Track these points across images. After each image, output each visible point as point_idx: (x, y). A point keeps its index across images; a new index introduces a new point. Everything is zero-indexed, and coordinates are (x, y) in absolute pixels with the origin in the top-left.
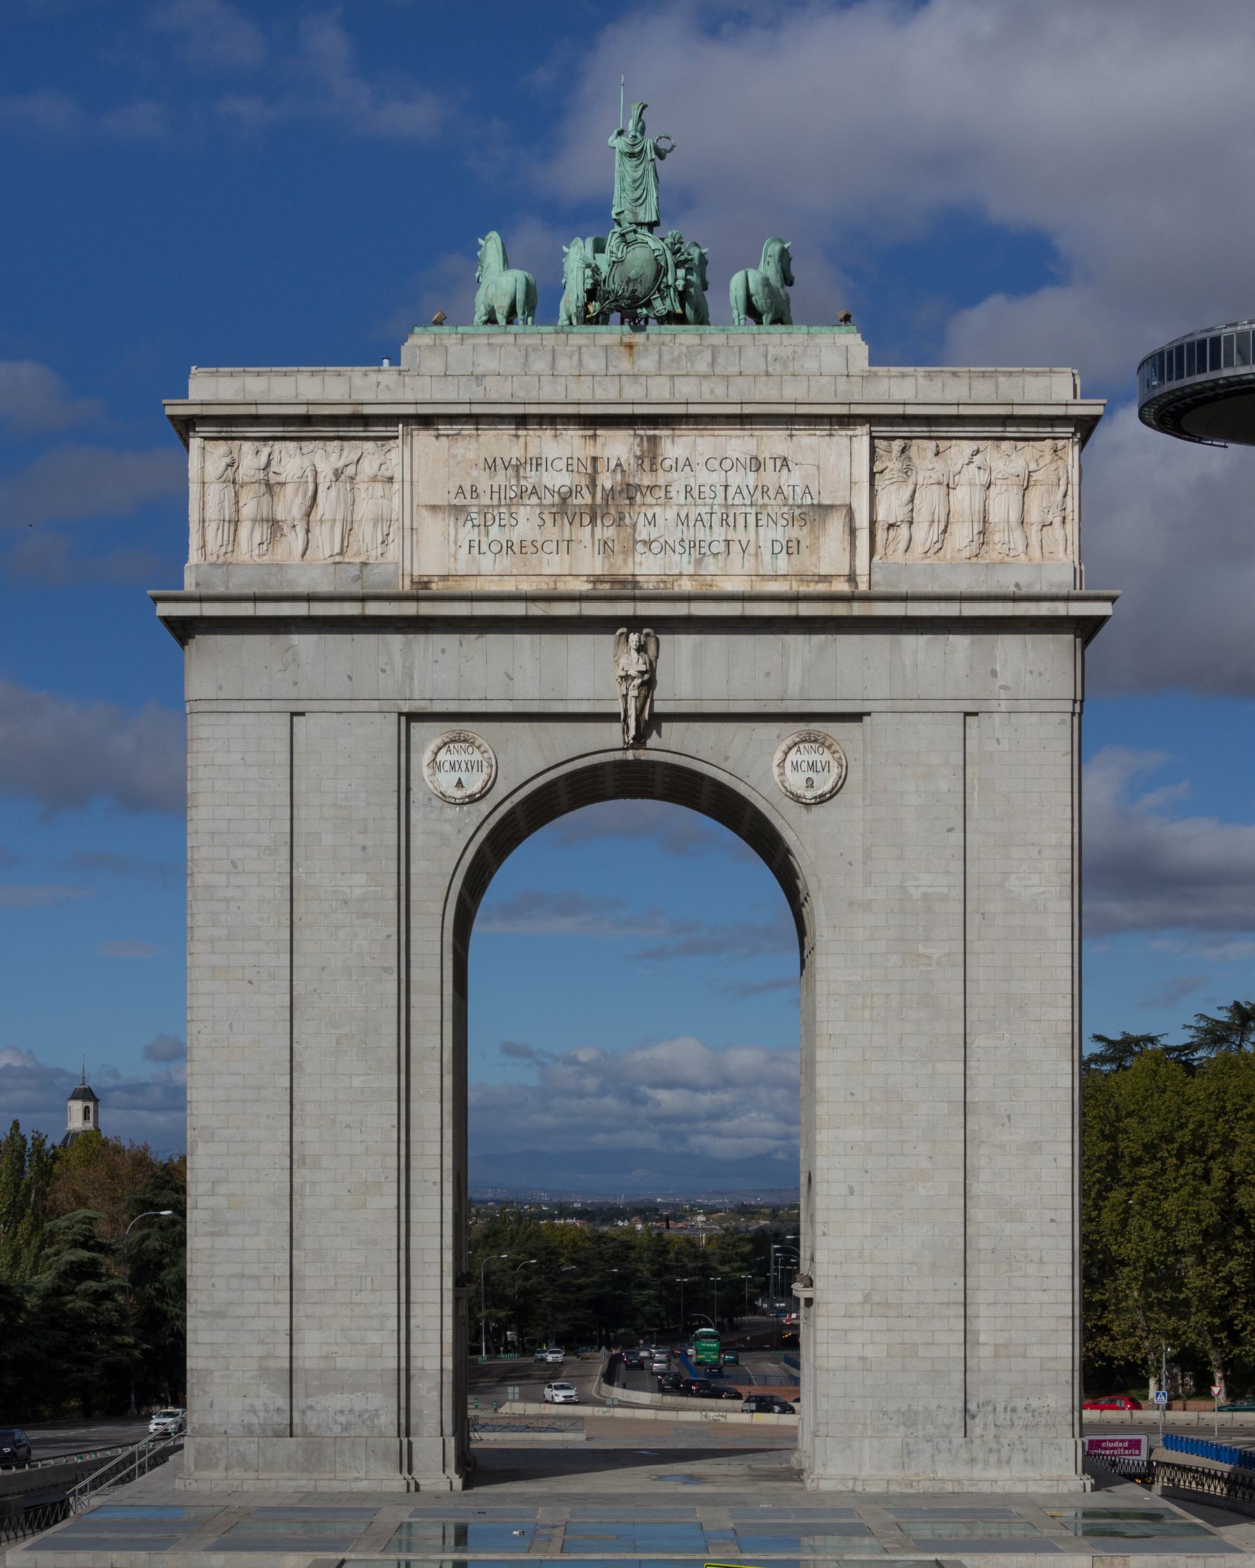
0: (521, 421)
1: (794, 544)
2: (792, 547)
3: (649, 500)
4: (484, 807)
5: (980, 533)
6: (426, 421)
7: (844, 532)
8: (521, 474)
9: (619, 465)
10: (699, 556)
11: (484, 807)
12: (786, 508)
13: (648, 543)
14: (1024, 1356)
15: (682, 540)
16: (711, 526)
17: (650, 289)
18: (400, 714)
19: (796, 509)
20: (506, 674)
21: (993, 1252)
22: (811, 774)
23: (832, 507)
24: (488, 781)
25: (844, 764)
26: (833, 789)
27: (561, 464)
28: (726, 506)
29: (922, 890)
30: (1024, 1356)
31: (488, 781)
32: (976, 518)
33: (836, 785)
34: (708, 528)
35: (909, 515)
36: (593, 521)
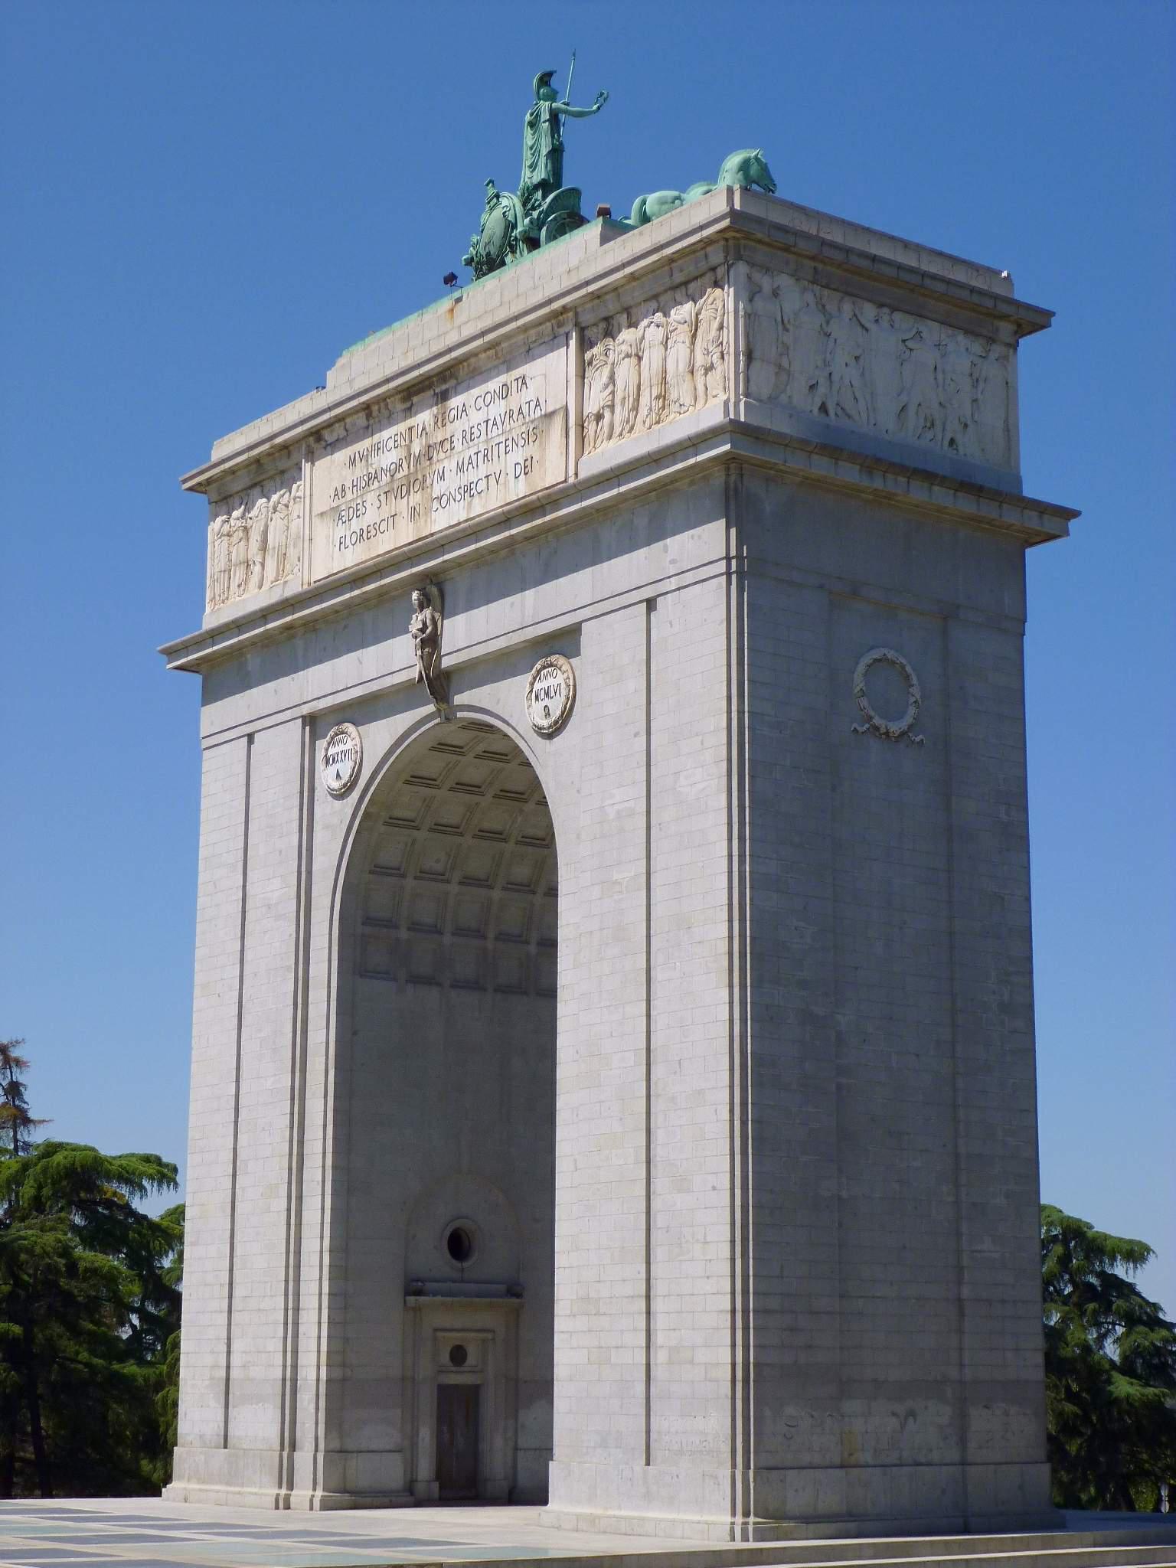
0: (367, 408)
1: (530, 460)
2: (527, 468)
3: (442, 455)
4: (356, 794)
5: (658, 397)
6: (317, 434)
7: (561, 436)
8: (370, 463)
9: (424, 429)
10: (470, 499)
11: (356, 794)
12: (524, 427)
13: (439, 498)
14: (692, 1362)
15: (460, 488)
16: (477, 466)
17: (501, 247)
18: (303, 717)
19: (530, 424)
20: (358, 659)
21: (667, 1232)
22: (547, 702)
23: (553, 413)
24: (354, 768)
25: (571, 683)
26: (563, 713)
27: (391, 443)
28: (487, 441)
29: (616, 807)
30: (692, 1362)
31: (354, 768)
32: (654, 381)
33: (565, 708)
34: (475, 467)
35: (610, 397)
36: (408, 492)
